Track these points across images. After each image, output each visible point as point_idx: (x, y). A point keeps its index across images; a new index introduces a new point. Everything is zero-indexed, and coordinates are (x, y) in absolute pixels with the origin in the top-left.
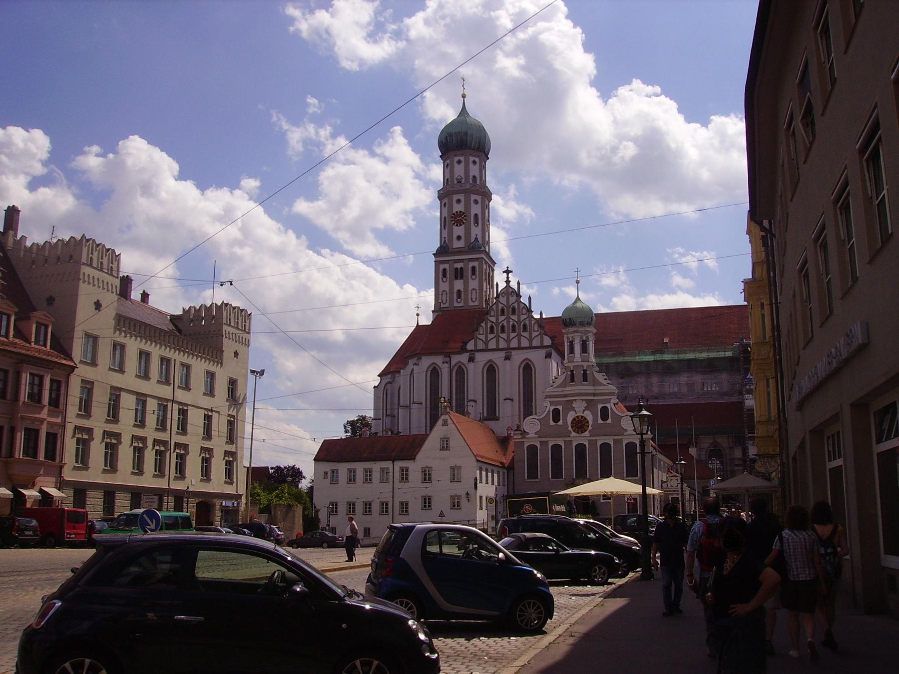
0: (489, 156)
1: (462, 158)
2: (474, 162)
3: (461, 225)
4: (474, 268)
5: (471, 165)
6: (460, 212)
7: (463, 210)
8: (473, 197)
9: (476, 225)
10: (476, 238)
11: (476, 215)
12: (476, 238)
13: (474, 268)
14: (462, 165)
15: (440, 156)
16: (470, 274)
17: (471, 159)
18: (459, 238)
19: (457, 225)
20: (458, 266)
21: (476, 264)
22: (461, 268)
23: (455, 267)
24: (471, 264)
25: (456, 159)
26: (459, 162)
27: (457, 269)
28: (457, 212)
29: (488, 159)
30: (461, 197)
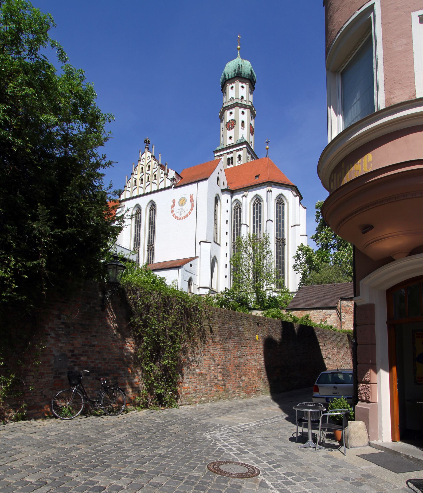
0: (255, 86)
1: (234, 85)
2: (243, 87)
3: (232, 129)
4: (240, 156)
5: (240, 88)
6: (232, 120)
7: (234, 119)
8: (241, 110)
9: (243, 128)
10: (243, 137)
11: (243, 122)
12: (243, 137)
13: (240, 156)
14: (234, 89)
15: (222, 90)
16: (237, 159)
17: (241, 84)
18: (231, 138)
19: (230, 130)
20: (230, 156)
21: (241, 153)
22: (232, 158)
23: (227, 158)
24: (238, 153)
25: (230, 86)
26: (232, 88)
27: (229, 159)
28: (230, 121)
29: (254, 88)
30: (233, 110)
